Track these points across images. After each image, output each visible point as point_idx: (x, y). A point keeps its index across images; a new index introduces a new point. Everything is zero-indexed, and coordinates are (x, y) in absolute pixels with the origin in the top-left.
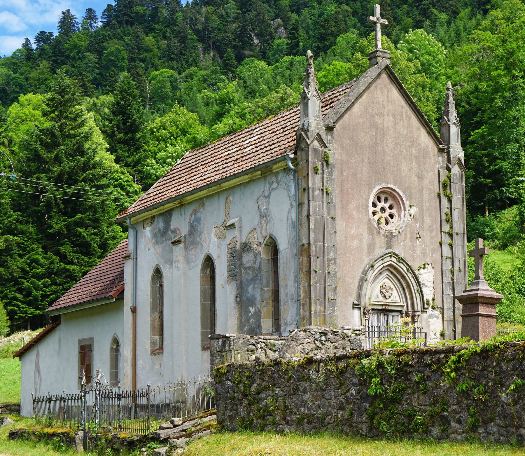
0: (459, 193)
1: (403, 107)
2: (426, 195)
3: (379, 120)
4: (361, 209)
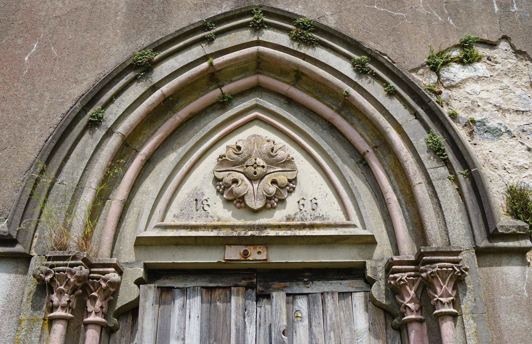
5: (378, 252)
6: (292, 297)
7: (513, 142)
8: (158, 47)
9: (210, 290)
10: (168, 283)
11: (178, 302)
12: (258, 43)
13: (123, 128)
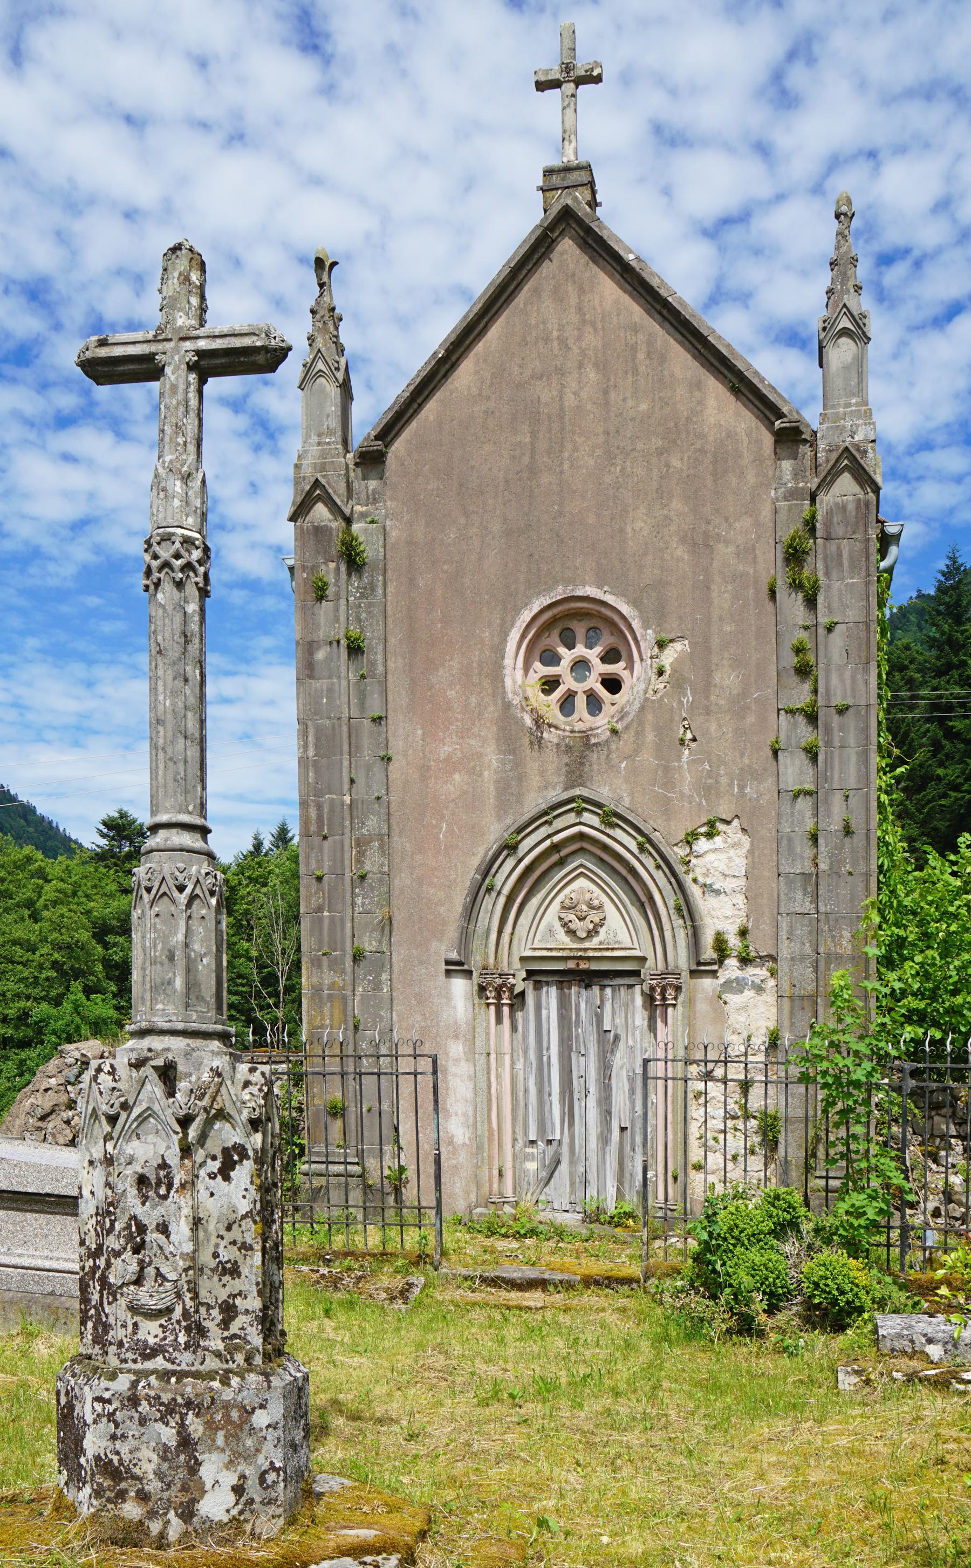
0: (853, 567)
1: (635, 329)
2: (722, 598)
3: (545, 393)
4: (475, 680)
5: (648, 964)
6: (603, 988)
7: (726, 899)
8: (519, 831)
9: (561, 982)
10: (538, 978)
11: (545, 989)
12: (580, 823)
13: (506, 890)
